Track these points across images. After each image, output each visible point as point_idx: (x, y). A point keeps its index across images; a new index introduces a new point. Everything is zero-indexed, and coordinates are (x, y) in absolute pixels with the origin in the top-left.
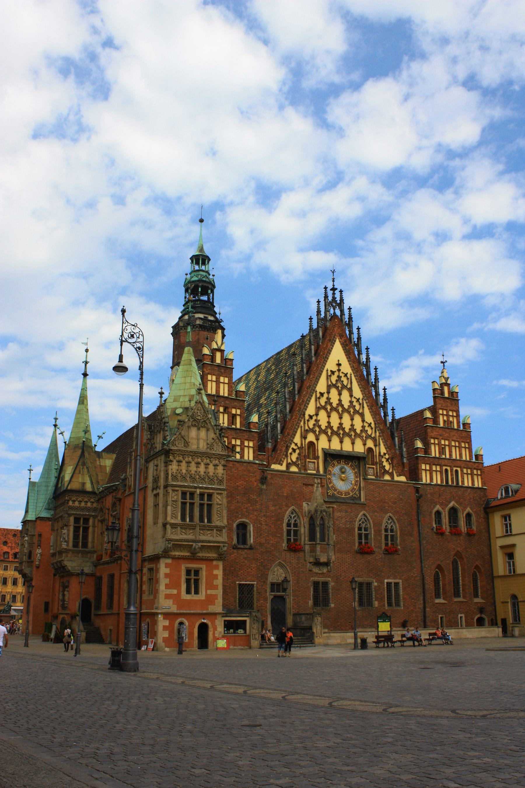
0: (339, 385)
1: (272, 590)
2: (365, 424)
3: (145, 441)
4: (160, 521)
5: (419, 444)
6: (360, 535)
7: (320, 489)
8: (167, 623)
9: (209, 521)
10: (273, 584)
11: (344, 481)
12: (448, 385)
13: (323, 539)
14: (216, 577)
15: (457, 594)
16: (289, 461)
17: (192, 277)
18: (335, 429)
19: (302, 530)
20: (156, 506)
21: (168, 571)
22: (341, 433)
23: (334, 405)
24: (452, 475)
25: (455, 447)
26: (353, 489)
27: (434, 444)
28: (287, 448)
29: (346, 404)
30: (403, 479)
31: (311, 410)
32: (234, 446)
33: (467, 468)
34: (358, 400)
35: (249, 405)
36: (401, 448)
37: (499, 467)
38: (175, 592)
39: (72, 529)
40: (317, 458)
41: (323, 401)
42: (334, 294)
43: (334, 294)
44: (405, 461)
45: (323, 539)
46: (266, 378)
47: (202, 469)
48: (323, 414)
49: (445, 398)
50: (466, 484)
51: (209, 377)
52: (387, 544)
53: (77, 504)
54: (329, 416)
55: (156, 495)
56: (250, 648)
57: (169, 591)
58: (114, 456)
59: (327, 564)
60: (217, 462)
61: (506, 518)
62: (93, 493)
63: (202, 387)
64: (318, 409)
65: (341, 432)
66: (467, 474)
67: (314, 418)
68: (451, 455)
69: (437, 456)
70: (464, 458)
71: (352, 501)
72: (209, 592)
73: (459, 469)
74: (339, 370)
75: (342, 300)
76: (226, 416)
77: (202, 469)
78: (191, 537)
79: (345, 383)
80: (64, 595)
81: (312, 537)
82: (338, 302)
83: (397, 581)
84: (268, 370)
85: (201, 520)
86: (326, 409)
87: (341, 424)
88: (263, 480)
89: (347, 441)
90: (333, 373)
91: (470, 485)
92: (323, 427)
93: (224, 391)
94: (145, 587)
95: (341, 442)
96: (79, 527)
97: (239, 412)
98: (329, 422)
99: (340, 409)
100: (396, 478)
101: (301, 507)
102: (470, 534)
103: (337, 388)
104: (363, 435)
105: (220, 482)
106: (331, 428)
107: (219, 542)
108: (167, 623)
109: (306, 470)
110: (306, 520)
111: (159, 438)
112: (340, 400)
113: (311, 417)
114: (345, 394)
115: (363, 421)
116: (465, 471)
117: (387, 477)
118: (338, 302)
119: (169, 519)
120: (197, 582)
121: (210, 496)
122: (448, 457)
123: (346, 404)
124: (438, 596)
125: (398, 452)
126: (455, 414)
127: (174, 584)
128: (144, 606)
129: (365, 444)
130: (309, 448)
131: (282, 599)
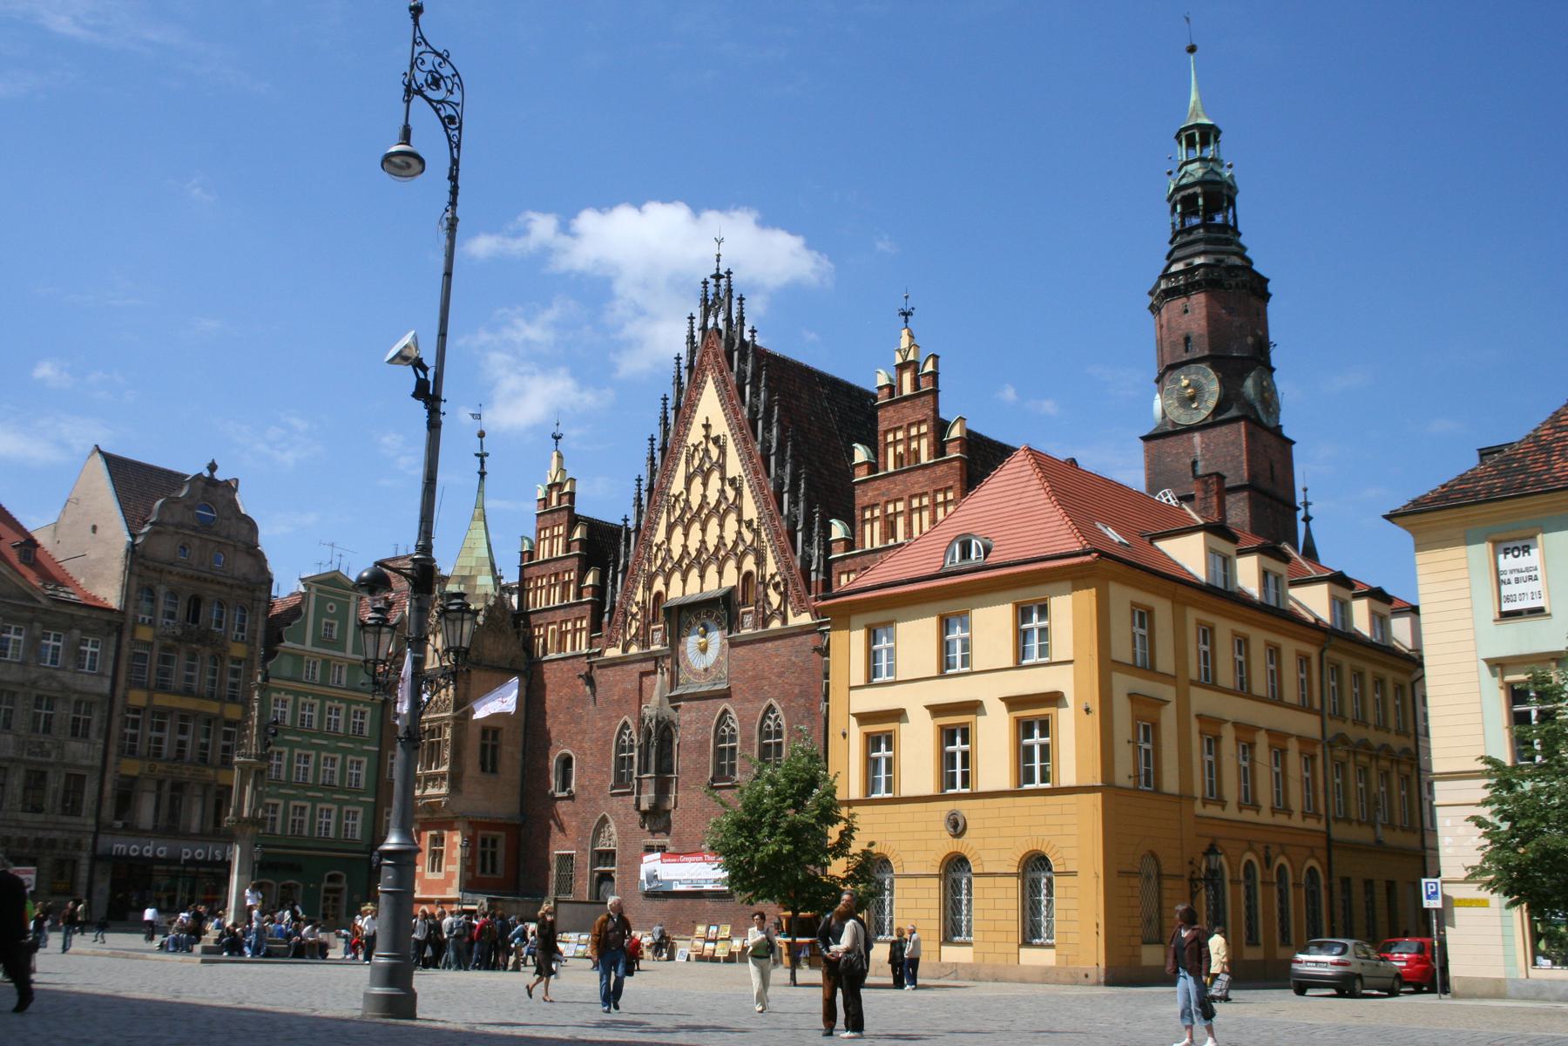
10: (601, 853)
30: (806, 619)
32: (563, 634)
42: (718, 286)
43: (718, 286)
64: (670, 529)
75: (729, 290)
89: (712, 570)
90: (696, 448)
98: (685, 547)
100: (793, 621)
112: (704, 496)
113: (659, 547)
115: (740, 521)
117: (776, 624)
125: (798, 562)
129: (739, 568)
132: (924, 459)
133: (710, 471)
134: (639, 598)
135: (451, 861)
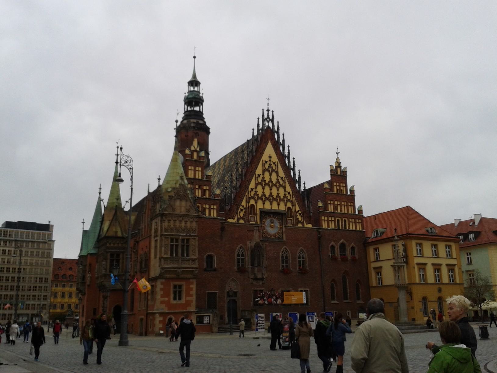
0: (270, 169)
1: (229, 296)
2: (287, 193)
3: (150, 207)
4: (158, 256)
5: (320, 204)
6: (283, 261)
7: (258, 233)
8: (161, 319)
9: (187, 255)
11: (272, 228)
12: (340, 167)
13: (259, 264)
14: (192, 289)
15: (346, 297)
16: (239, 216)
17: (188, 95)
18: (267, 196)
19: (247, 258)
20: (156, 247)
21: (162, 286)
22: (271, 199)
23: (267, 182)
24: (342, 223)
25: (344, 205)
26: (278, 233)
27: (330, 204)
28: (238, 209)
29: (274, 181)
31: (252, 185)
32: (205, 209)
33: (352, 219)
34: (282, 178)
35: (219, 181)
36: (309, 206)
37: (375, 217)
38: (166, 299)
39: (109, 261)
40: (256, 214)
41: (260, 180)
42: (268, 113)
43: (268, 113)
44: (311, 214)
45: (259, 264)
46: (229, 164)
47: (183, 224)
48: (260, 188)
49: (339, 175)
50: (351, 229)
51: (190, 168)
52: (300, 266)
53: (112, 245)
54: (263, 189)
55: (156, 241)
56: (213, 333)
57: (163, 299)
58: (136, 213)
59: (262, 279)
60: (192, 220)
61: (376, 249)
62: (123, 238)
63: (184, 175)
64: (257, 185)
65: (271, 198)
66: (352, 222)
67: (254, 190)
68: (341, 211)
69: (332, 211)
70: (350, 212)
71: (278, 240)
72: (188, 298)
73: (346, 219)
74: (270, 160)
75: (273, 117)
76: (200, 191)
77: (183, 224)
78: (176, 265)
79: (274, 168)
80: (104, 303)
81: (252, 263)
82: (271, 118)
83: (307, 289)
84: (231, 159)
85: (183, 254)
86: (262, 185)
87: (271, 193)
88: (223, 229)
90: (266, 162)
91: (354, 229)
92: (260, 196)
93: (199, 176)
94: (149, 297)
95: (271, 204)
96: (114, 260)
97: (208, 188)
98: (263, 193)
99: (271, 184)
100: (306, 226)
101: (246, 244)
102: (354, 259)
103: (269, 171)
104: (285, 200)
105: (194, 231)
106: (265, 196)
107: (192, 268)
108: (161, 319)
109: (249, 221)
110: (249, 252)
111: (158, 206)
112: (270, 179)
113: (252, 189)
114: (274, 174)
115: (285, 191)
116: (351, 220)
117: (300, 225)
118: (271, 118)
119: (163, 255)
120: (180, 293)
121: (188, 240)
122: (339, 211)
123: (274, 181)
124: (333, 299)
126: (344, 185)
127: (166, 294)
128: (149, 309)
129: (286, 205)
130: (251, 208)
131: (235, 302)
132: (345, 193)
133: (272, 171)
134: (244, 203)
135: (188, 295)
